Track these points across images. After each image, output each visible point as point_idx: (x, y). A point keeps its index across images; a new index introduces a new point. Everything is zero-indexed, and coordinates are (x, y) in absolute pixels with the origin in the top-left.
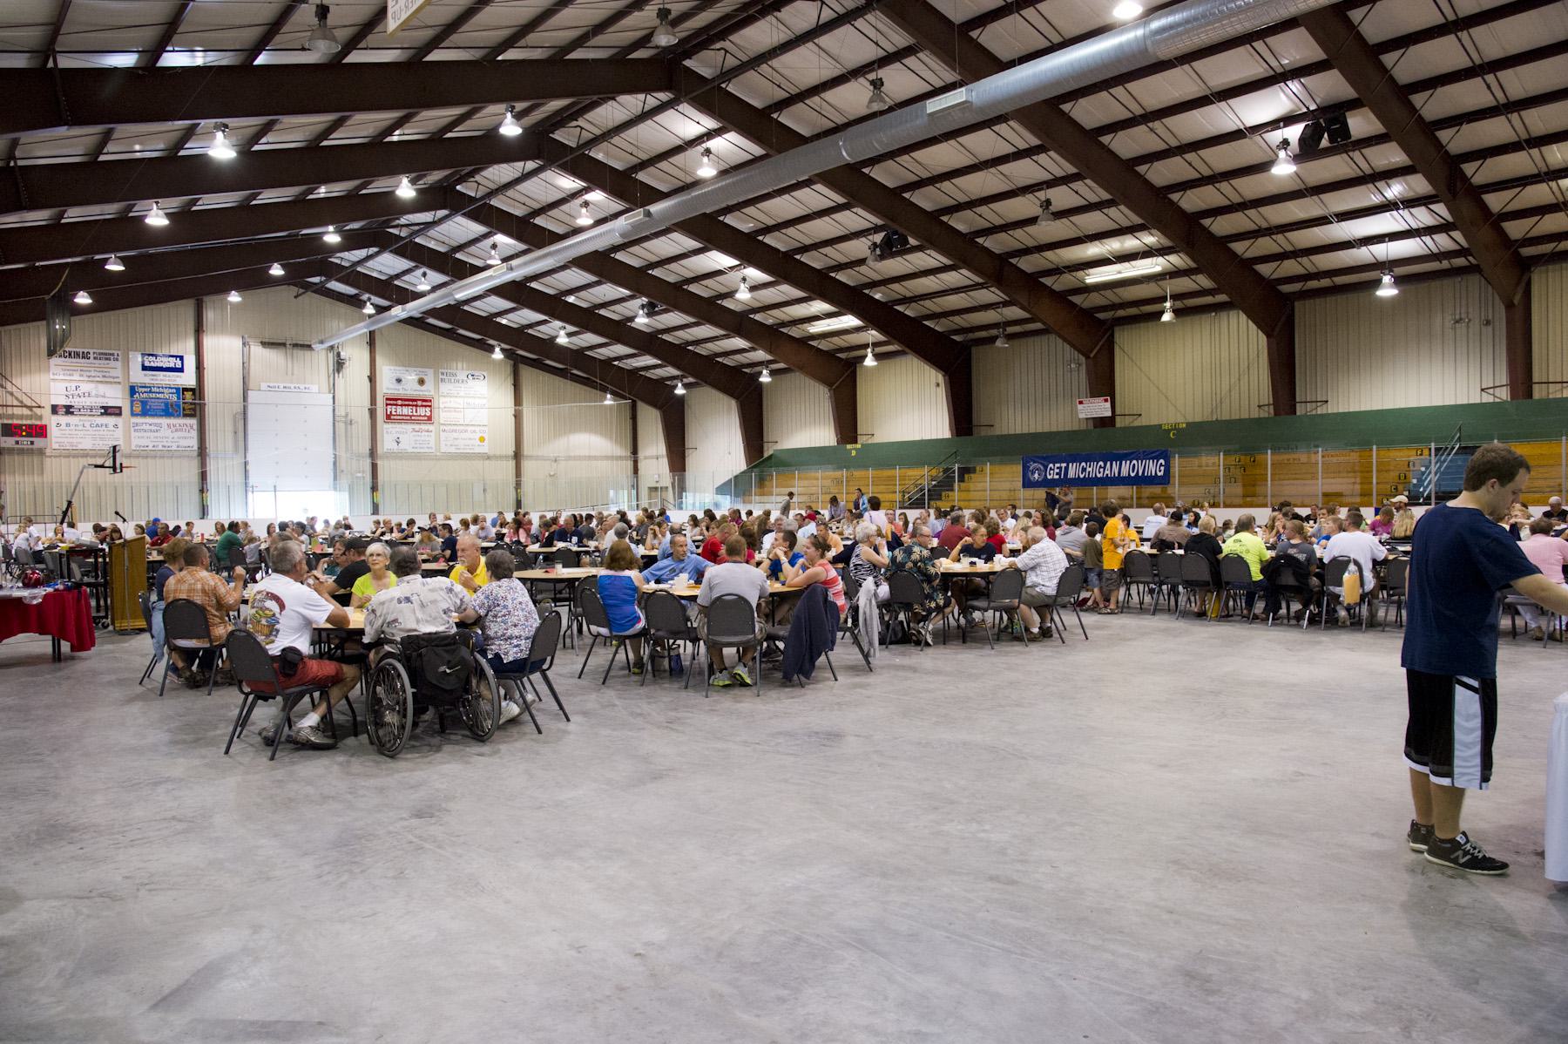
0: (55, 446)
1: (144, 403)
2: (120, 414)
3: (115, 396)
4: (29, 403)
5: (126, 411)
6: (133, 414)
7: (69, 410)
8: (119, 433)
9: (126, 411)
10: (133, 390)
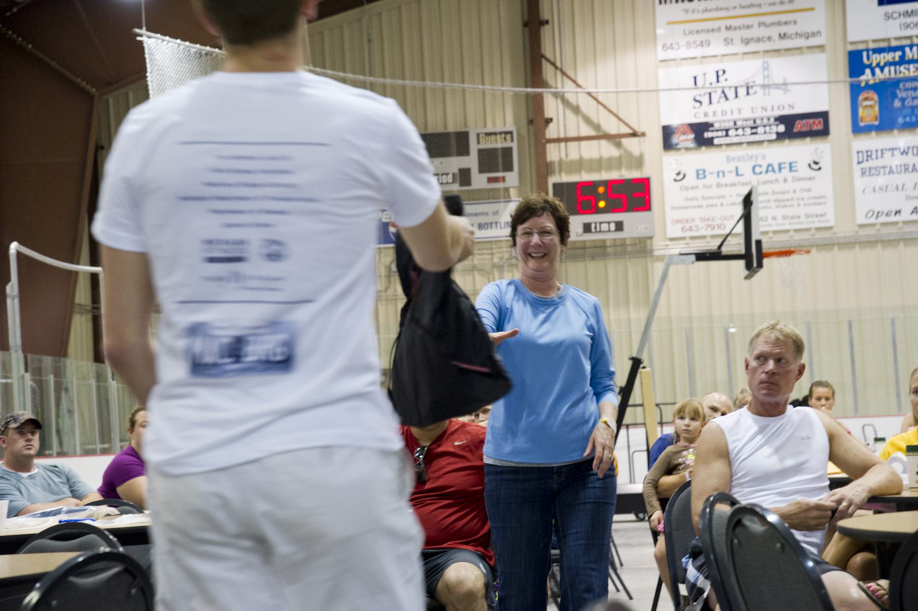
0: (674, 231)
1: (886, 90)
2: (824, 132)
3: (813, 86)
4: (611, 126)
5: (840, 122)
6: (858, 129)
7: (702, 134)
8: (823, 183)
9: (840, 122)
10: (856, 62)
